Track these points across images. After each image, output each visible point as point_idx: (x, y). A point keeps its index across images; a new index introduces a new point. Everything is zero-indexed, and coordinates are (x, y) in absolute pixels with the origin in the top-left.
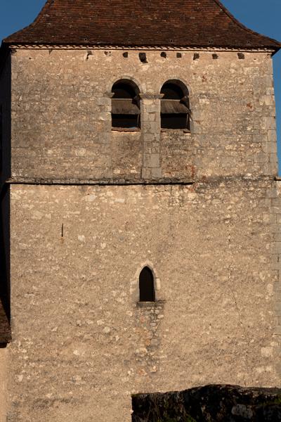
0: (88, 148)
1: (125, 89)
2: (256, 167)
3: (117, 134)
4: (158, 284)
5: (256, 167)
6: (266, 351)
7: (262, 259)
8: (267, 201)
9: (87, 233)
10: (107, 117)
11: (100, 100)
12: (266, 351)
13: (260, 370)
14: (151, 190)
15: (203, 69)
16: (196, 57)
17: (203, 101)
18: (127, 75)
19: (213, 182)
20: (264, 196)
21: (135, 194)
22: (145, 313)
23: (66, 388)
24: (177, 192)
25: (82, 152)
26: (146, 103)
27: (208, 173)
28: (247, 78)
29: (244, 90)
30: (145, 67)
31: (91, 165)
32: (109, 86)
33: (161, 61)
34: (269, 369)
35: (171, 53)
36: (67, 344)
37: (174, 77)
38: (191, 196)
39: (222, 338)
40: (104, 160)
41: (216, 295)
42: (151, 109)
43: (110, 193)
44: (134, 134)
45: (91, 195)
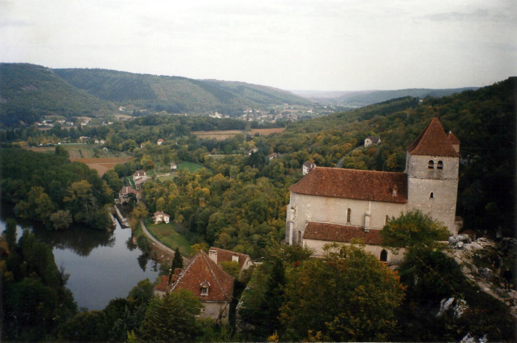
1: (431, 162)
3: (429, 170)
4: (434, 196)
6: (452, 208)
10: (427, 167)
12: (452, 208)
14: (434, 180)
19: (446, 179)
21: (431, 181)
24: (439, 181)
30: (435, 159)
38: (441, 181)
40: (426, 174)
42: (435, 166)
44: (432, 170)
45: (423, 180)
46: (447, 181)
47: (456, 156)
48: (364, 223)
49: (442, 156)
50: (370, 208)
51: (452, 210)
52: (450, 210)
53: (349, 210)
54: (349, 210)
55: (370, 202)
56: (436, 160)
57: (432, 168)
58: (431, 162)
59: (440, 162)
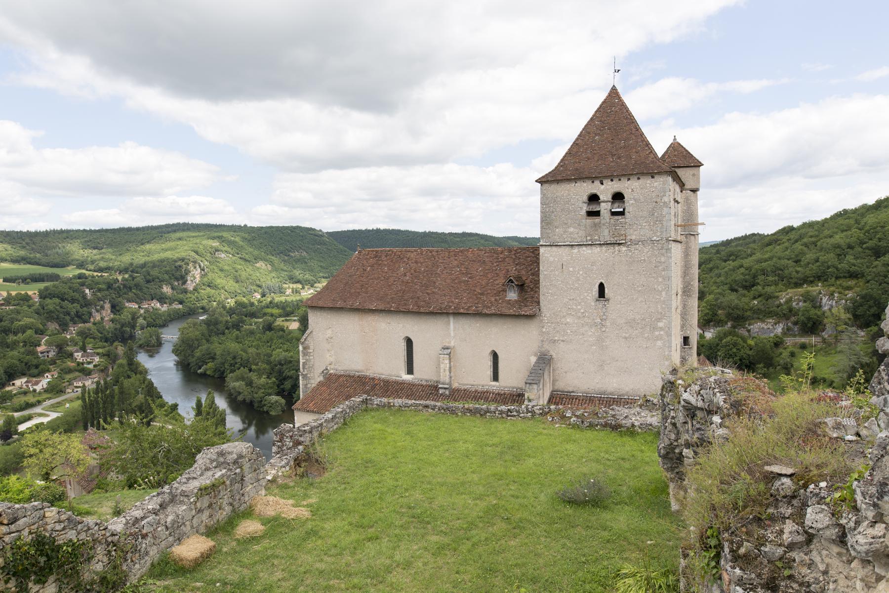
0: (574, 228)
1: (594, 198)
2: (659, 234)
5: (659, 234)
7: (660, 280)
8: (664, 251)
9: (574, 267)
10: (583, 212)
11: (581, 205)
12: (660, 324)
13: (657, 333)
14: (604, 248)
15: (630, 187)
16: (629, 179)
17: (631, 202)
18: (594, 191)
20: (662, 248)
21: (597, 250)
22: (600, 304)
23: (563, 336)
25: (571, 230)
26: (602, 204)
27: (633, 237)
28: (656, 188)
29: (654, 195)
30: (602, 187)
31: (576, 236)
32: (585, 198)
33: (610, 183)
34: (662, 333)
35: (616, 181)
36: (564, 317)
37: (617, 190)
38: (624, 249)
39: (638, 317)
40: (582, 233)
41: (635, 297)
42: (605, 208)
43: (584, 248)
44: (596, 220)
46: (640, 246)
47: (659, 173)
48: (438, 372)
49: (619, 177)
50: (452, 334)
51: (661, 329)
52: (655, 328)
53: (409, 342)
54: (409, 342)
55: (451, 319)
56: (605, 190)
57: (597, 214)
58: (594, 198)
59: (618, 197)
